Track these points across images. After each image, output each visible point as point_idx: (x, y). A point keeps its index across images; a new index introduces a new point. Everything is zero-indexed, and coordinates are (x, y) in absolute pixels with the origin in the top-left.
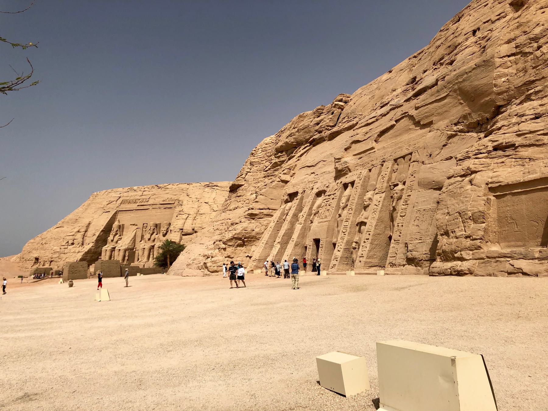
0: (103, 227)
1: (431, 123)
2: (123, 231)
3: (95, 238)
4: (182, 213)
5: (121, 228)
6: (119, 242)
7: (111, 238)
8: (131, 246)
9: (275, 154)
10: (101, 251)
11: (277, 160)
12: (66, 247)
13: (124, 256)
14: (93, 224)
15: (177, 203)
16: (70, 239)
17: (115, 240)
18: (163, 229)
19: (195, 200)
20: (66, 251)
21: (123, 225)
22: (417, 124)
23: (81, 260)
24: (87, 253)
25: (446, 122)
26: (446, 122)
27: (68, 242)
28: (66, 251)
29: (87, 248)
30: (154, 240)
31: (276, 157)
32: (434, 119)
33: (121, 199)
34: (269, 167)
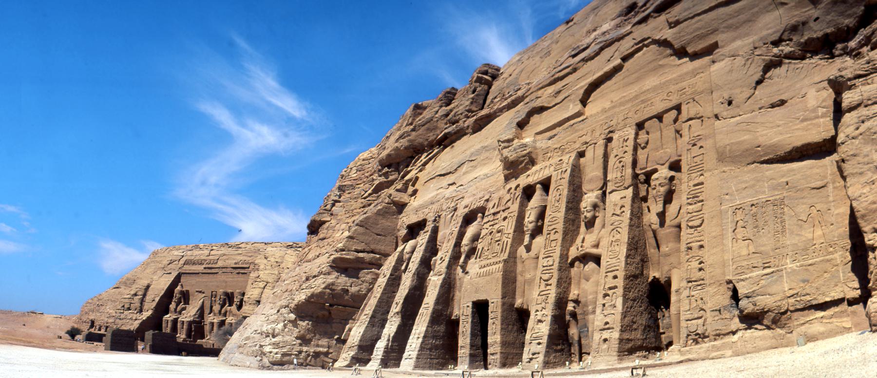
1: (715, 46)
7: (172, 306)
9: (380, 171)
11: (383, 179)
22: (681, 53)
25: (749, 41)
26: (749, 41)
31: (380, 176)
32: (720, 38)
33: (184, 259)
34: (370, 192)
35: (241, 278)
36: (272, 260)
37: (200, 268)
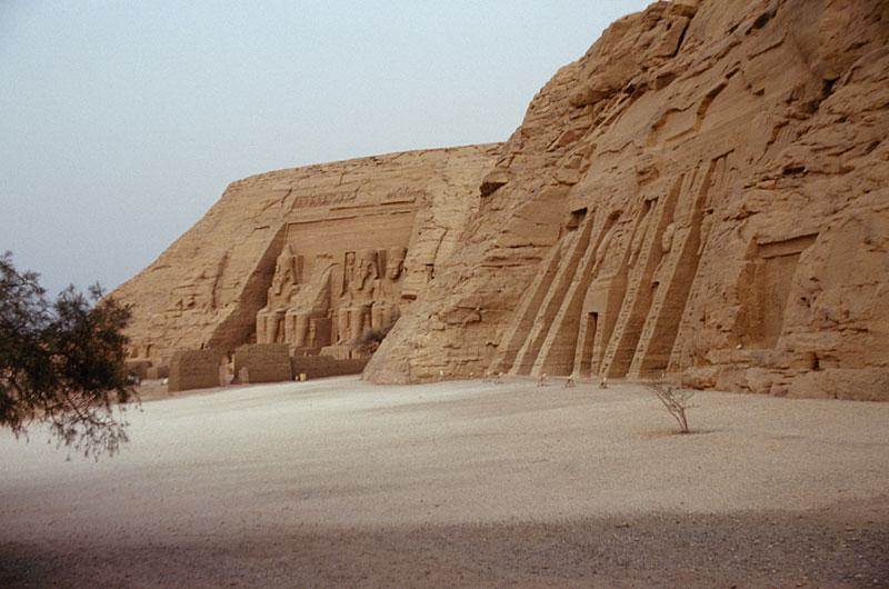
0: (256, 265)
2: (301, 272)
3: (240, 290)
4: (432, 225)
5: (297, 265)
6: (293, 298)
8: (320, 306)
10: (255, 319)
12: (178, 313)
13: (307, 331)
14: (233, 257)
15: (420, 199)
16: (184, 295)
17: (286, 293)
18: (391, 266)
19: (463, 189)
20: (180, 322)
21: (301, 258)
23: (213, 343)
24: (223, 326)
27: (181, 302)
28: (180, 322)
29: (224, 313)
30: (372, 292)
35: (400, 222)
36: (458, 182)
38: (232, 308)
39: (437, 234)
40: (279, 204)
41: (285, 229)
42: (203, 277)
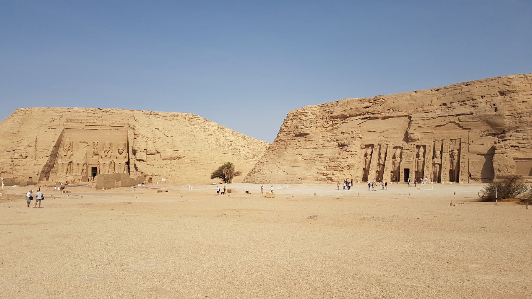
12: (21, 160)
15: (126, 127)
37: (83, 126)
38: (47, 159)
39: (145, 139)
40: (58, 120)
41: (63, 131)
42: (29, 146)
